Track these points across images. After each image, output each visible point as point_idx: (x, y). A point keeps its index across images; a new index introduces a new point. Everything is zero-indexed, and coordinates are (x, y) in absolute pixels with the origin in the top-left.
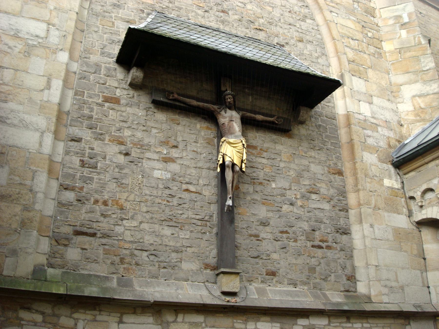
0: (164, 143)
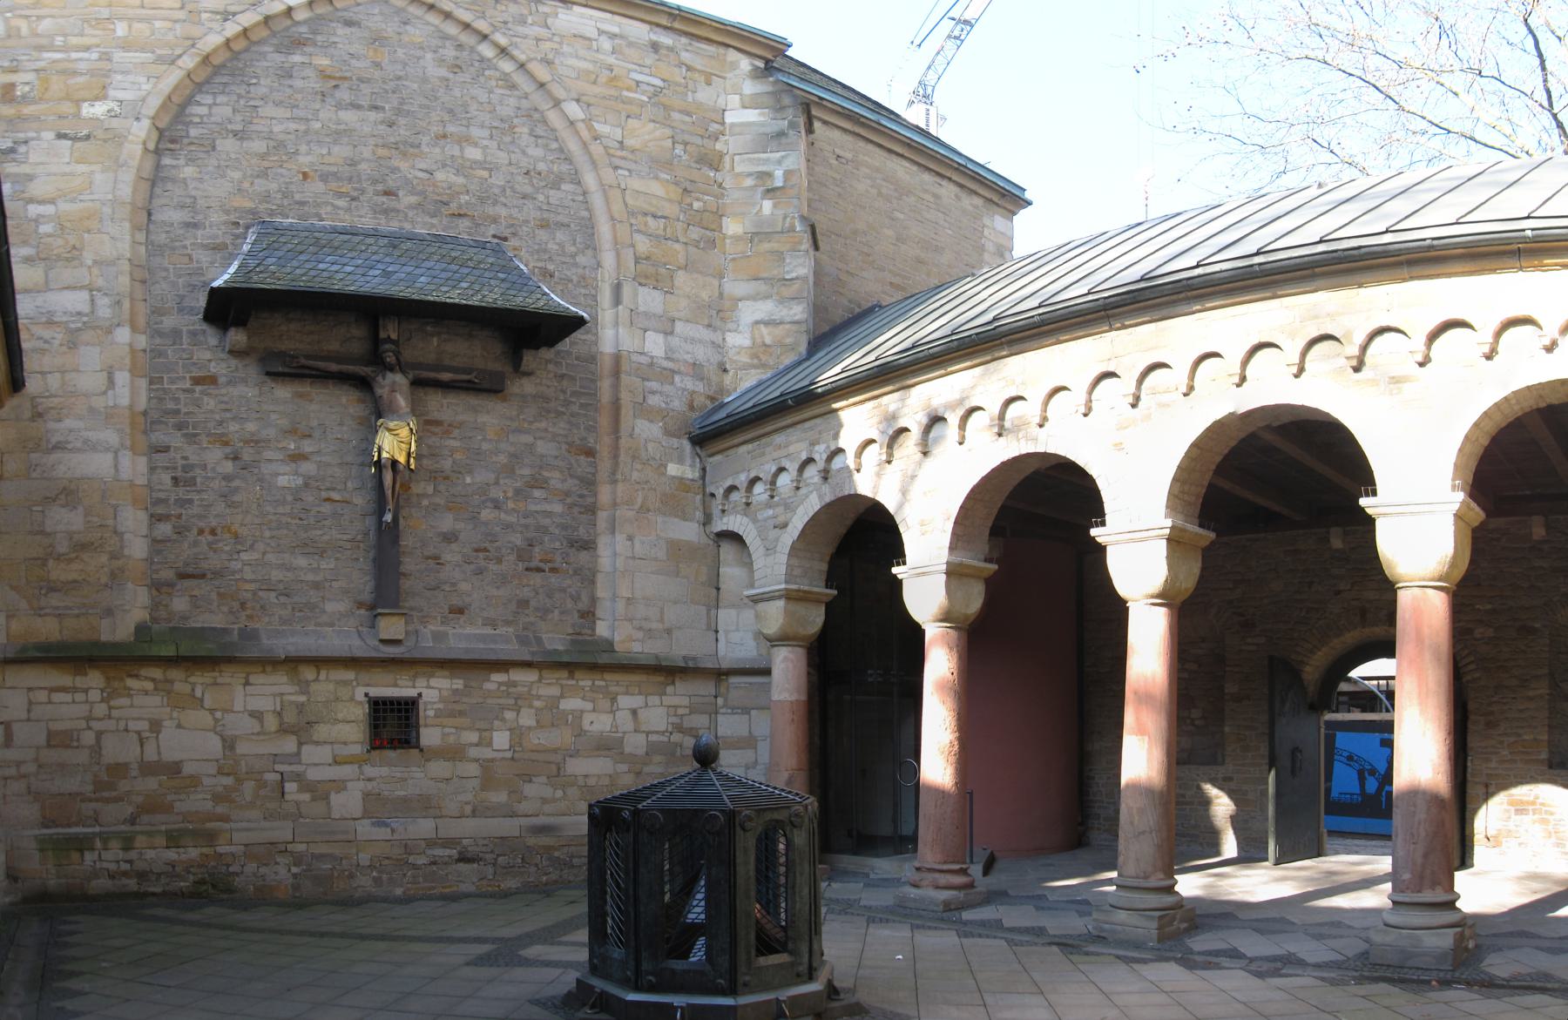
0: (292, 432)
